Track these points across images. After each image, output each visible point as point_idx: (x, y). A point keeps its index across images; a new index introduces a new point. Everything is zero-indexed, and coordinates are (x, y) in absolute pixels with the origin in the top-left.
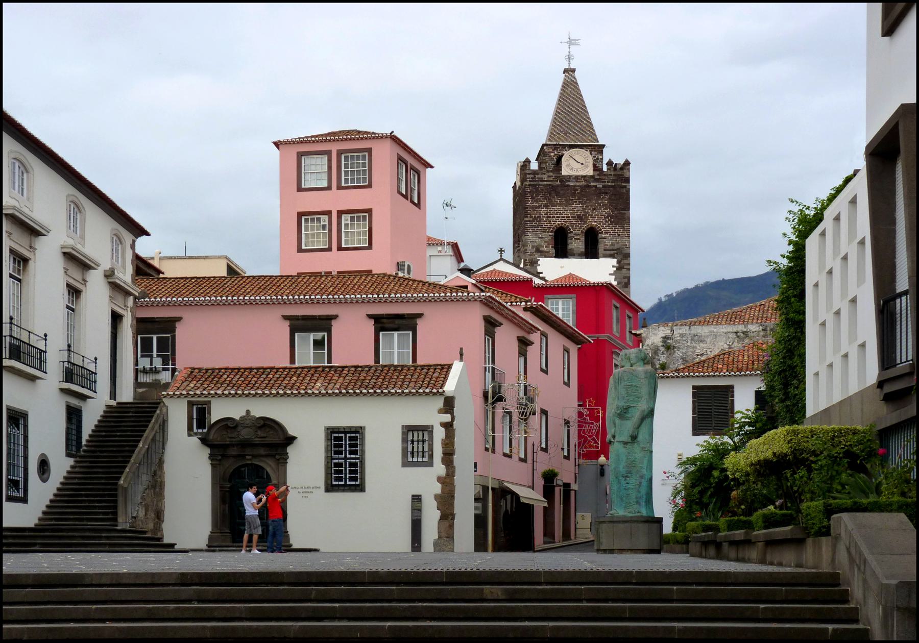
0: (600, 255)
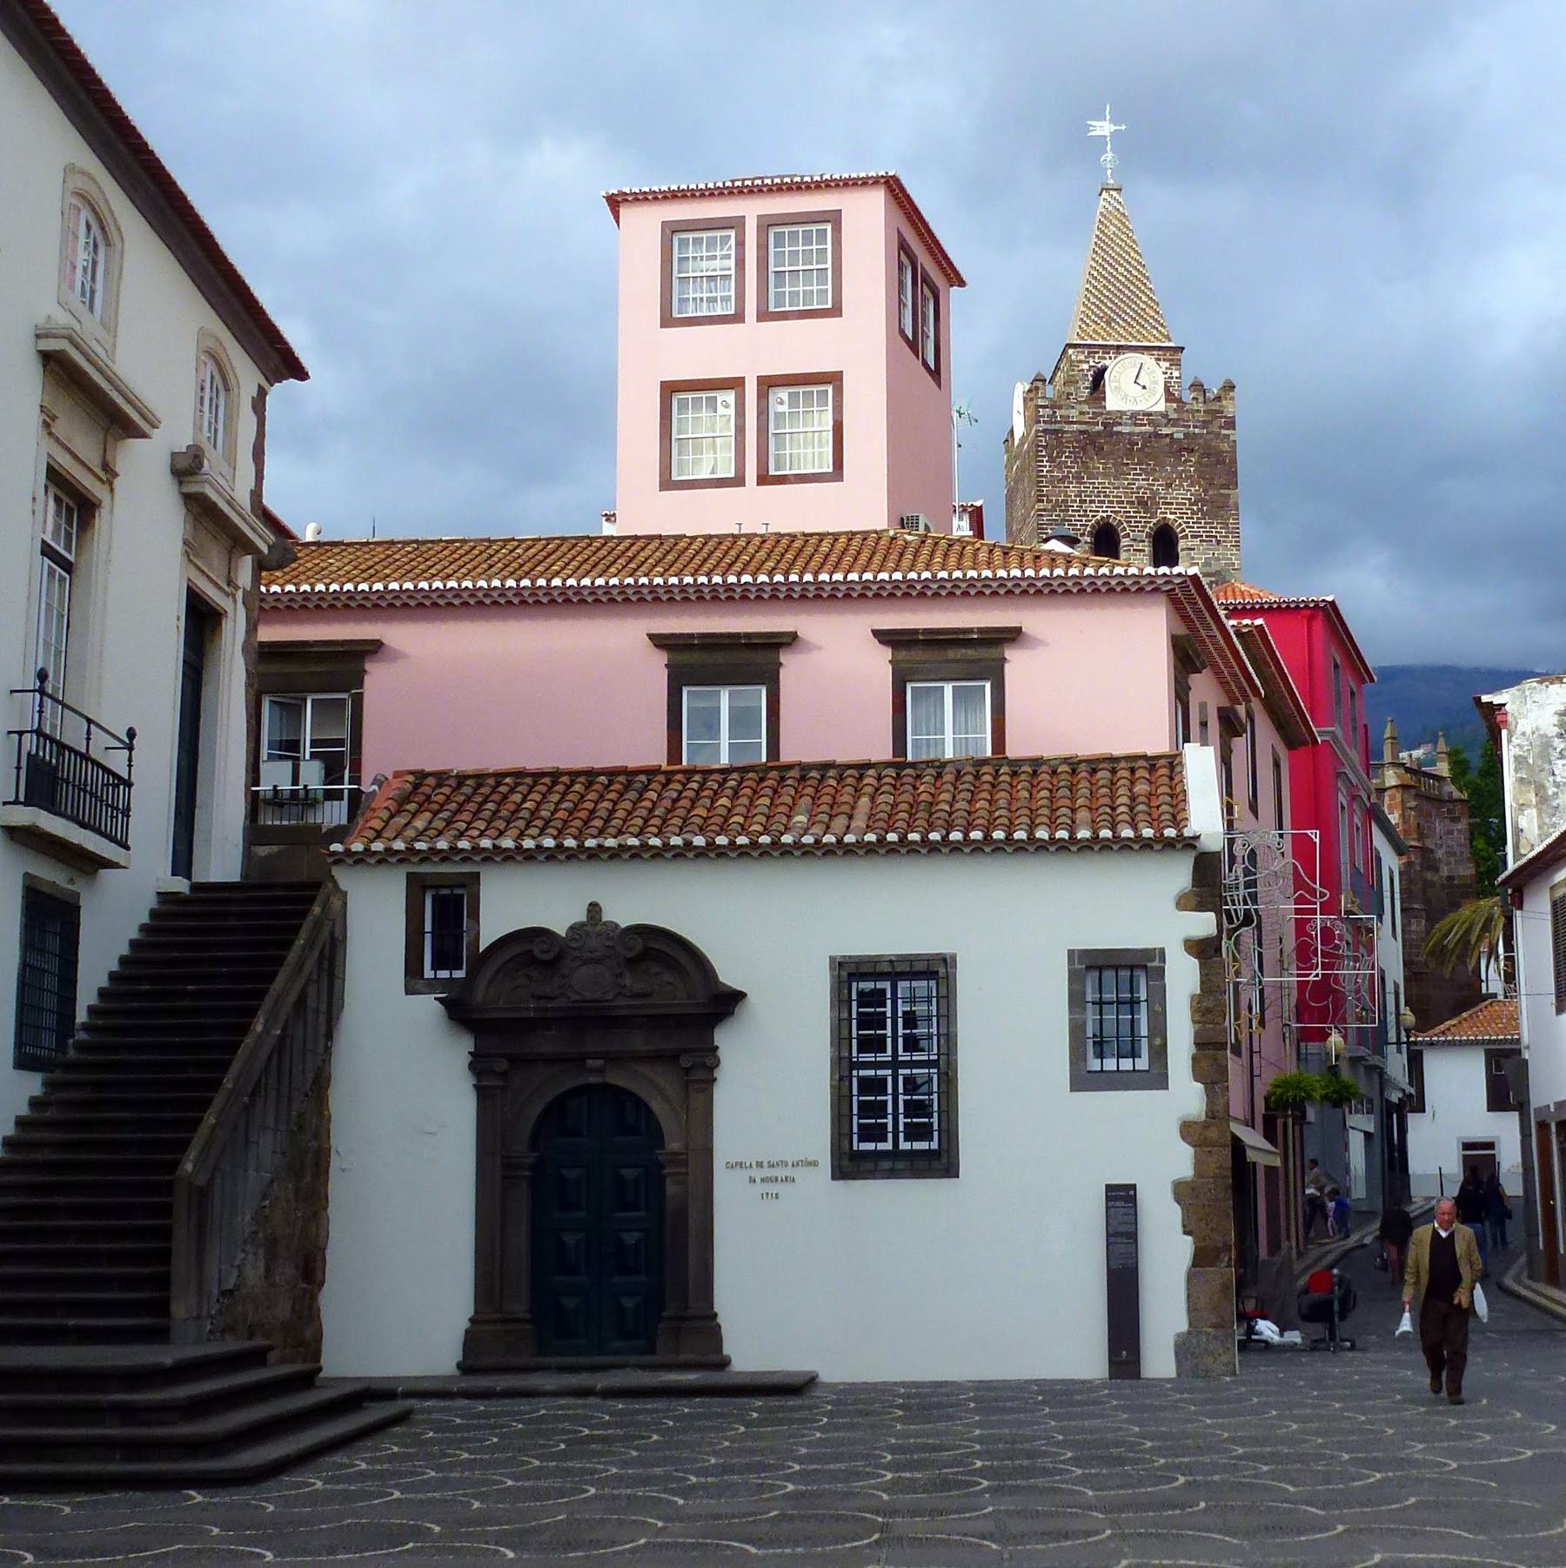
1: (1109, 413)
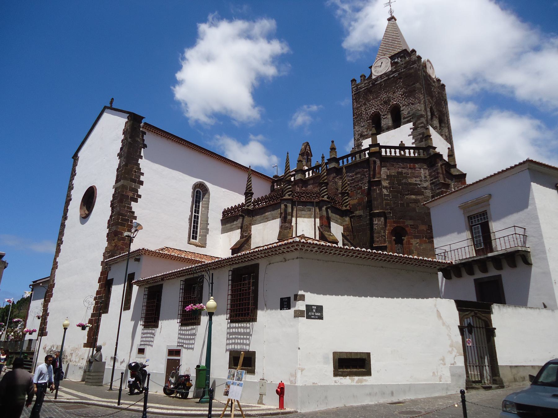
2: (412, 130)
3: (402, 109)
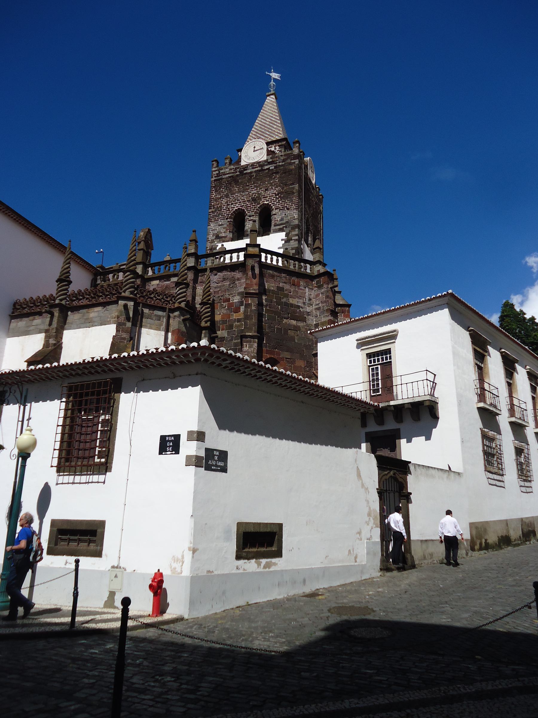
0: (272, 231)
1: (242, 166)
2: (283, 242)
3: (274, 212)
